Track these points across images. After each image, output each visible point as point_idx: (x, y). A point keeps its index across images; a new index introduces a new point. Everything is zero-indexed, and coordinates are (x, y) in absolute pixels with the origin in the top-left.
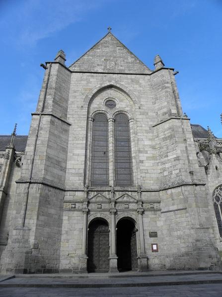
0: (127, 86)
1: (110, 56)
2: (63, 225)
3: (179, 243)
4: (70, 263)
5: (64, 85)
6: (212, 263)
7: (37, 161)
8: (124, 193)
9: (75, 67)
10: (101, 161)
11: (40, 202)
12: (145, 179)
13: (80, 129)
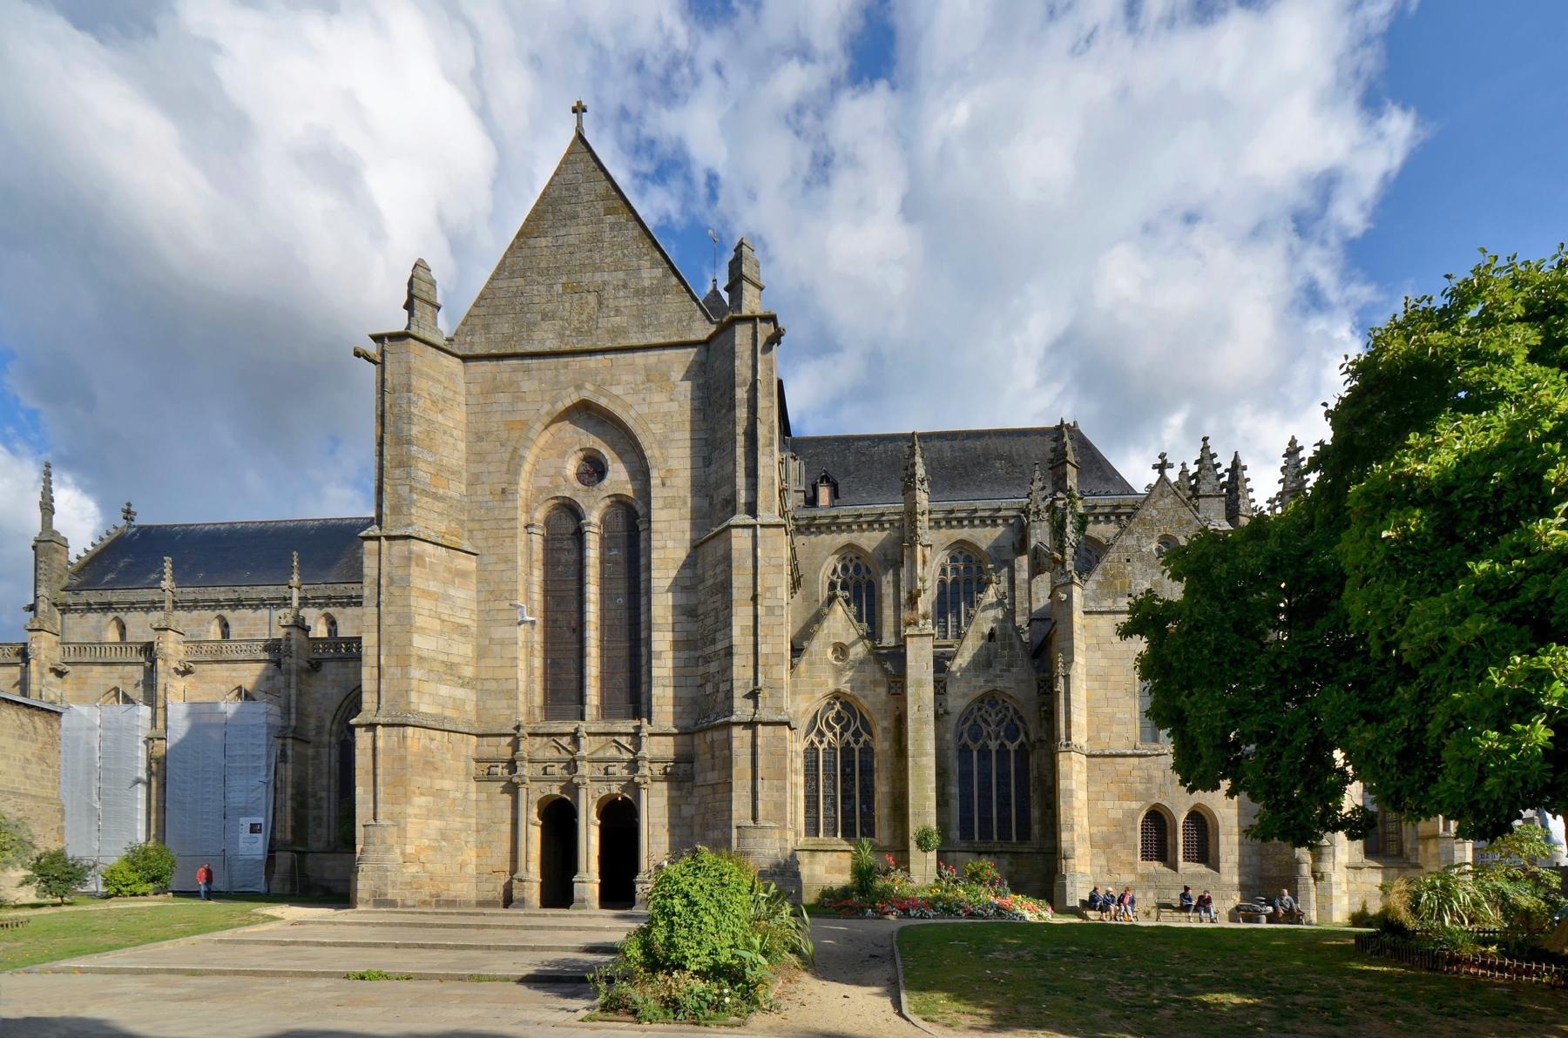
0: (629, 399)
5: (440, 418)
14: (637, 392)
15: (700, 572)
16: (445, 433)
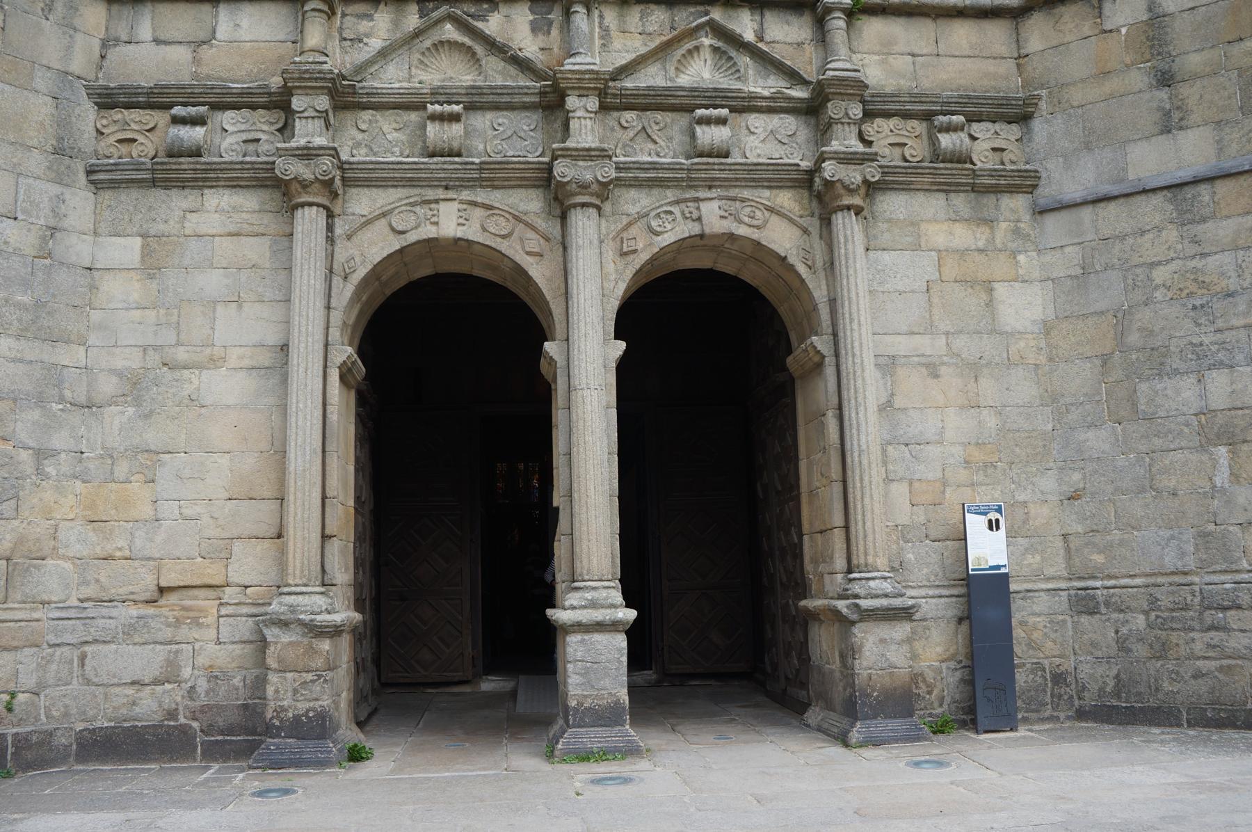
3: (1222, 478)
4: (169, 676)
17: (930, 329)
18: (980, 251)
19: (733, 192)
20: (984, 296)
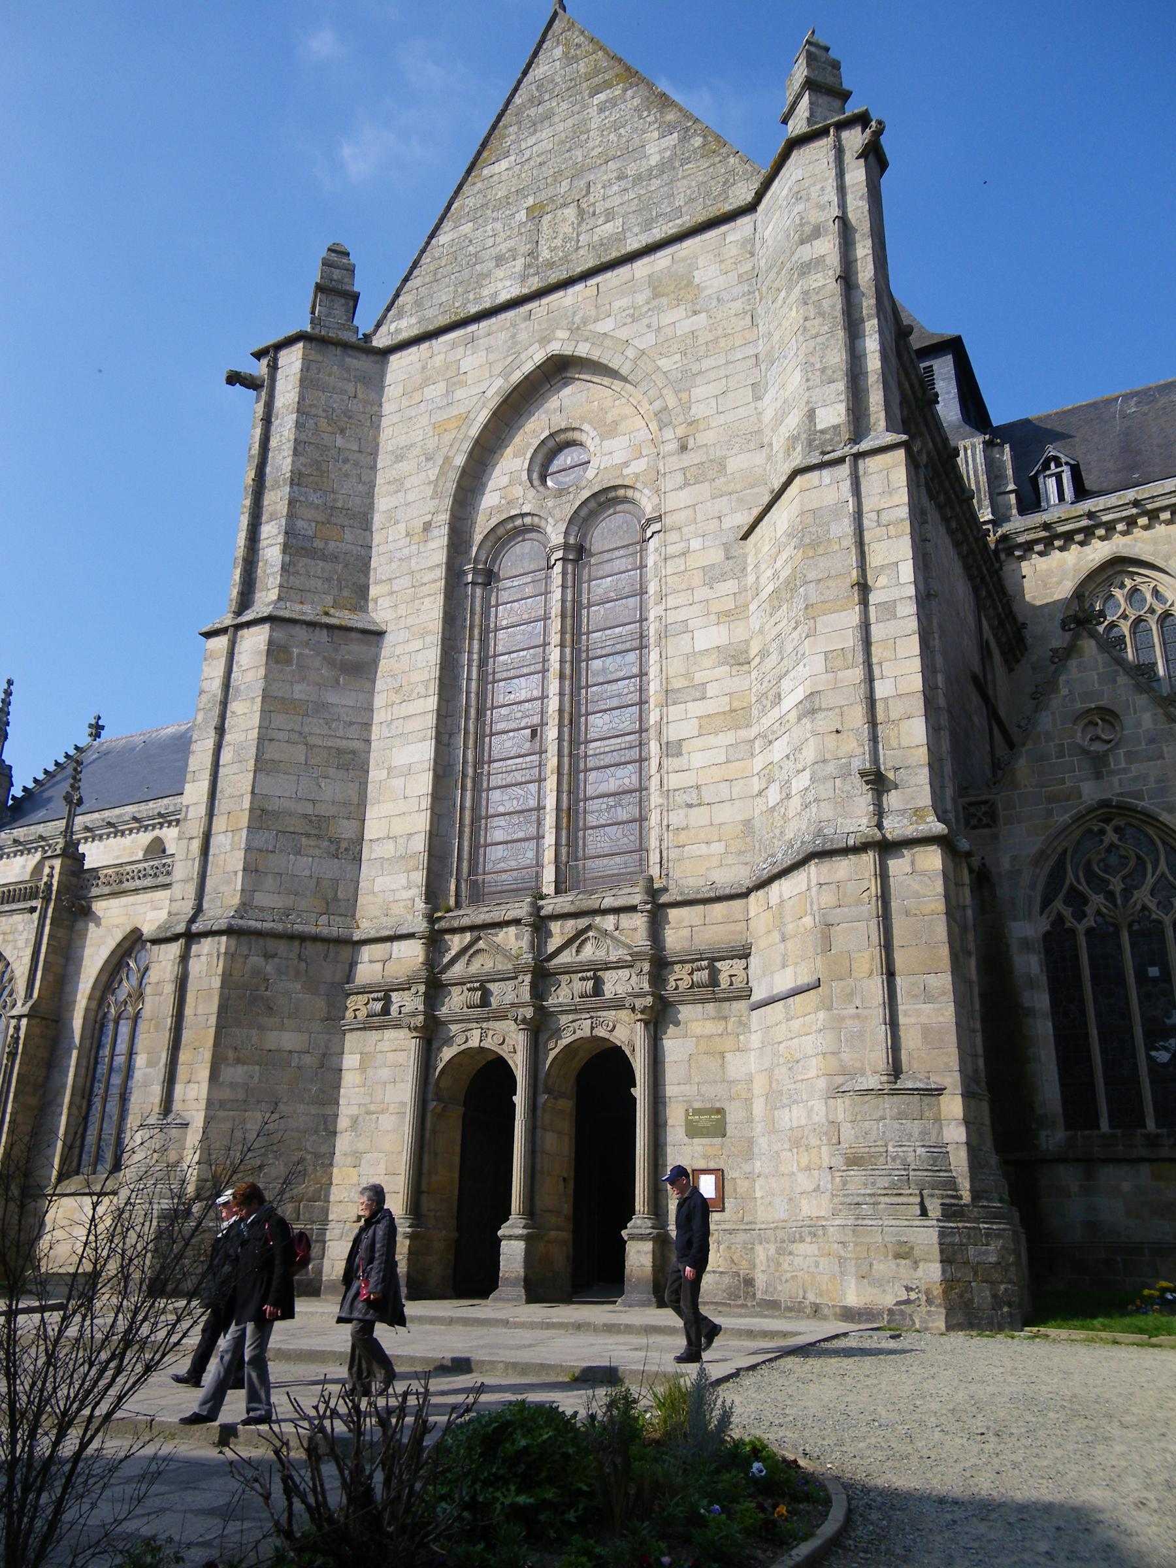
0: (623, 334)
1: (558, 175)
2: (342, 1090)
3: (795, 1169)
5: (340, 442)
6: (908, 1289)
7: (220, 842)
8: (582, 923)
9: (400, 316)
10: (518, 777)
11: (223, 1010)
12: (683, 837)
13: (416, 645)
14: (634, 319)
15: (751, 579)
16: (346, 461)
17: (689, 1081)
18: (721, 1035)
19: (599, 1014)
20: (720, 1061)
